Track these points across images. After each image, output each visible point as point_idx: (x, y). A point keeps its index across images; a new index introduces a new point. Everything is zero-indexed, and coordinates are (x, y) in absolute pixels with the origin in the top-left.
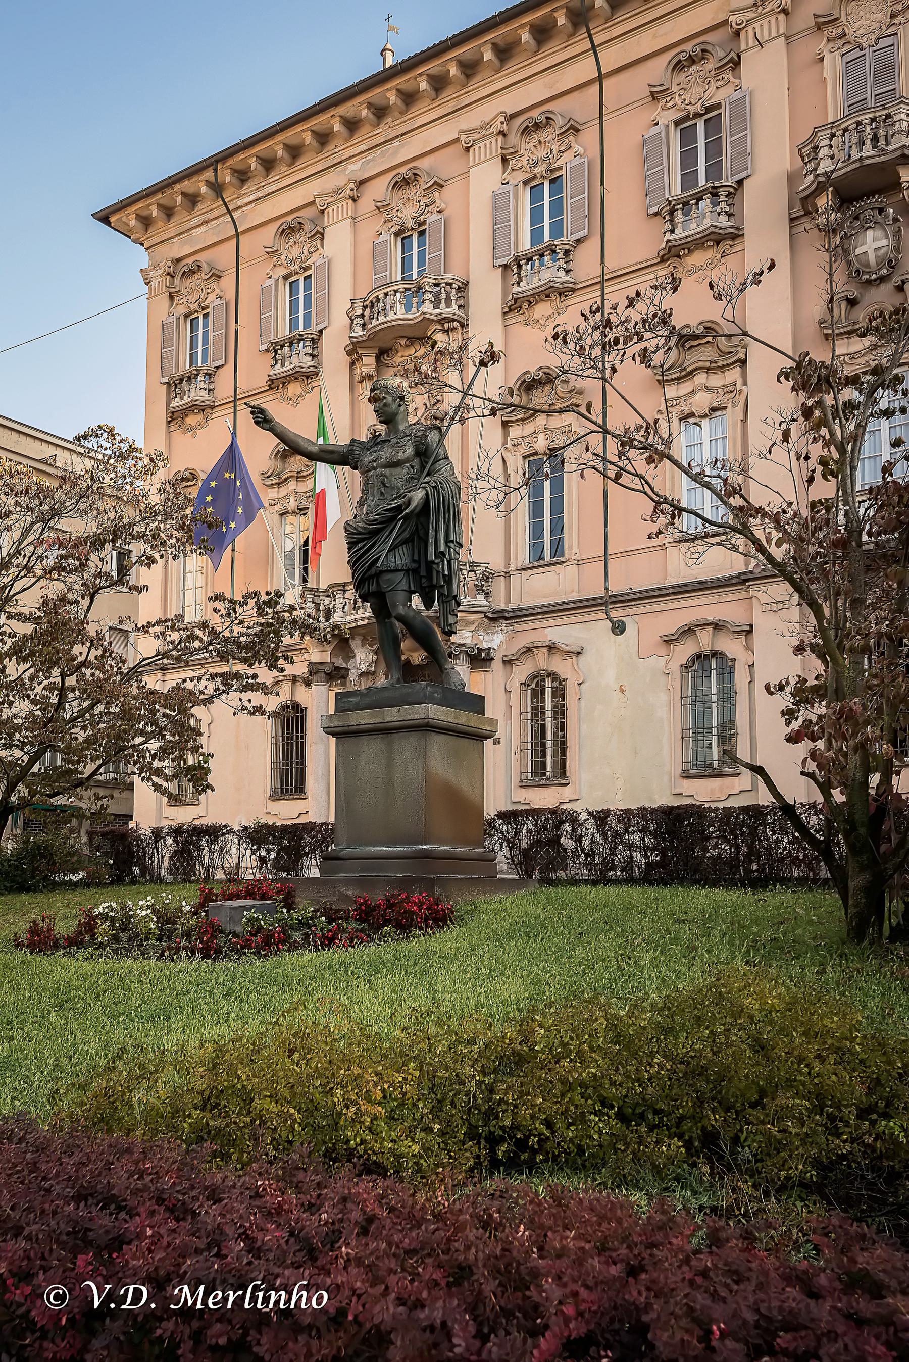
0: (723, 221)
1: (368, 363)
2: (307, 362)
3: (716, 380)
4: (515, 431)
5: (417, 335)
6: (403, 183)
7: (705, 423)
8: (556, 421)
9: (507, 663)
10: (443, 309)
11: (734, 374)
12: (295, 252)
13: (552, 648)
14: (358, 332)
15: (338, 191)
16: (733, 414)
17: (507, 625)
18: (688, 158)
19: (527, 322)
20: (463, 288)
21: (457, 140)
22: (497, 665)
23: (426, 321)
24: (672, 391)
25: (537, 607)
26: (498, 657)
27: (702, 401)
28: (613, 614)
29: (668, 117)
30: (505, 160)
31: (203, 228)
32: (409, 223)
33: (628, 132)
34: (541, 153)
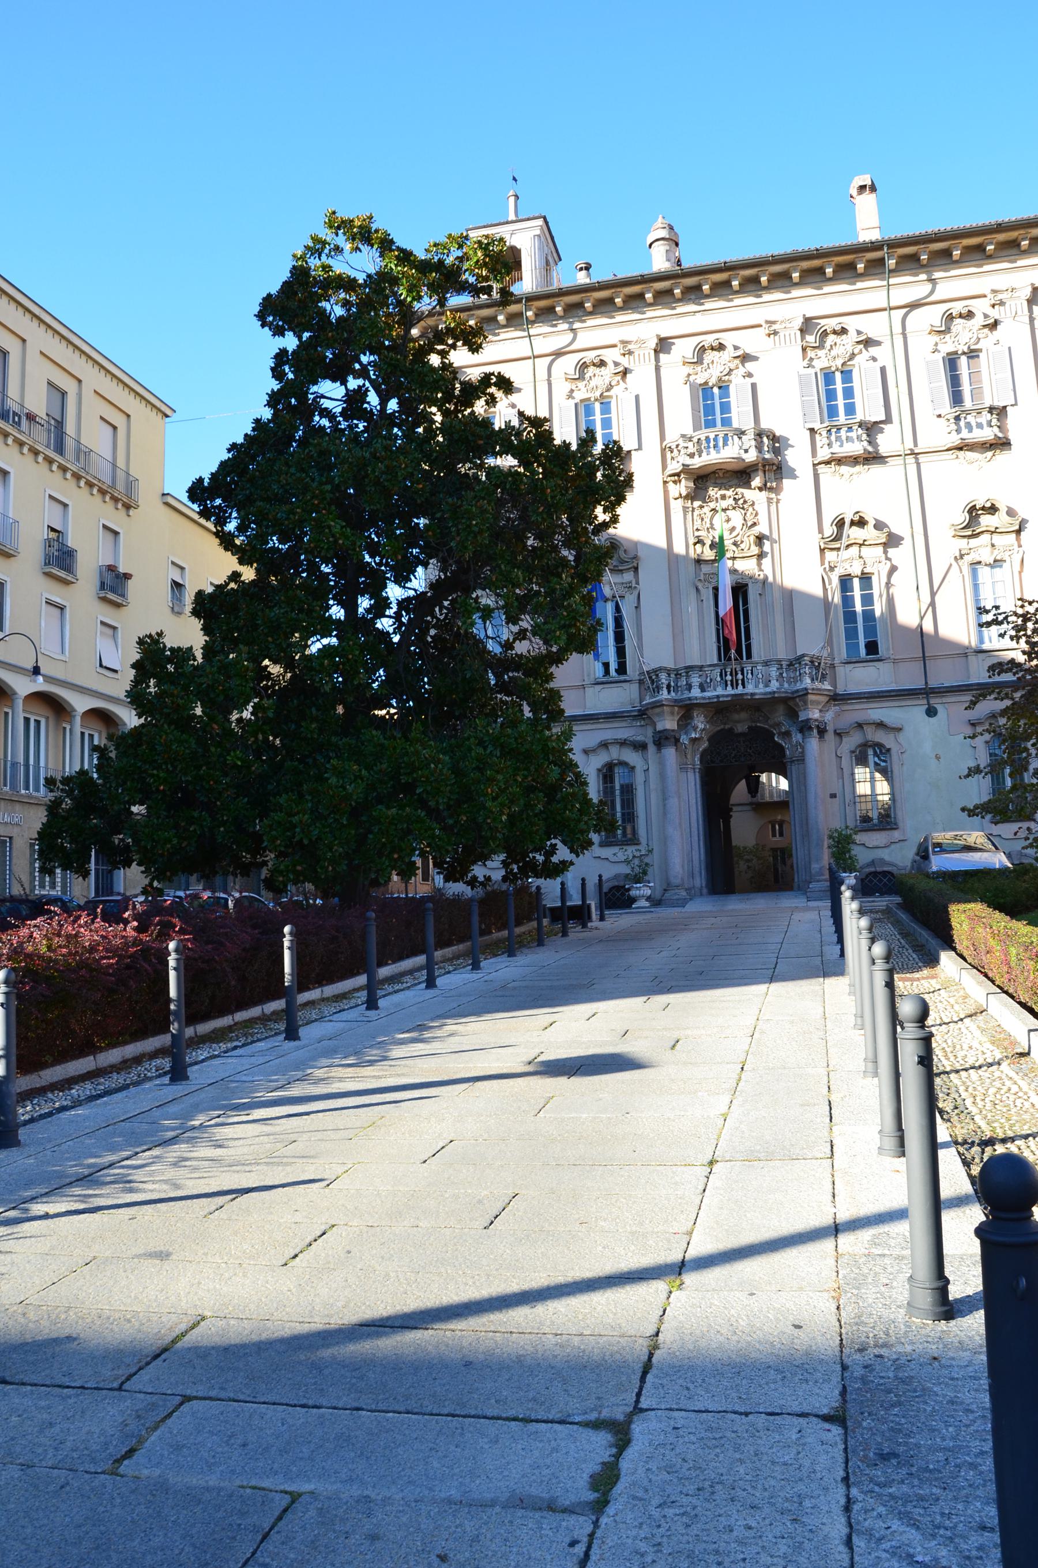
9: (839, 734)
13: (881, 725)
17: (835, 705)
22: (830, 736)
25: (865, 693)
26: (830, 728)
28: (932, 701)
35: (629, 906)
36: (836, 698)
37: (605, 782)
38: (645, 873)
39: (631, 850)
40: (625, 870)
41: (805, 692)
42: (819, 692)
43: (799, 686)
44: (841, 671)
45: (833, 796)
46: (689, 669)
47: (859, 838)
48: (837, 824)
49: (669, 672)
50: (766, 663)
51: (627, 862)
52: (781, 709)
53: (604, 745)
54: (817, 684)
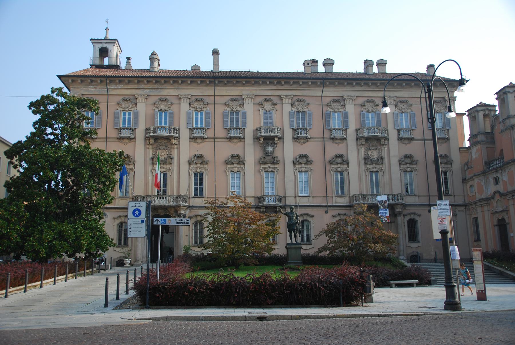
0: (241, 135)
1: (152, 141)
2: (132, 136)
3: (239, 166)
4: (192, 166)
5: (168, 139)
6: (161, 100)
7: (235, 174)
8: (202, 166)
10: (175, 135)
11: (242, 166)
12: (127, 106)
14: (152, 134)
15: (141, 96)
16: (242, 174)
18: (232, 119)
19: (195, 142)
20: (179, 129)
21: (178, 95)
23: (172, 136)
24: (229, 166)
27: (236, 169)
29: (228, 109)
30: (190, 104)
31: (94, 89)
32: (163, 110)
33: (220, 109)
34: (199, 106)
35: (123, 266)
36: (189, 208)
37: (119, 228)
38: (129, 256)
39: (125, 249)
40: (123, 255)
41: (180, 206)
42: (184, 206)
43: (178, 204)
44: (191, 199)
45: (187, 236)
46: (148, 196)
47: (192, 248)
48: (187, 244)
49: (141, 196)
50: (170, 196)
51: (124, 252)
52: (173, 210)
53: (120, 217)
54: (184, 204)
